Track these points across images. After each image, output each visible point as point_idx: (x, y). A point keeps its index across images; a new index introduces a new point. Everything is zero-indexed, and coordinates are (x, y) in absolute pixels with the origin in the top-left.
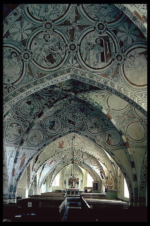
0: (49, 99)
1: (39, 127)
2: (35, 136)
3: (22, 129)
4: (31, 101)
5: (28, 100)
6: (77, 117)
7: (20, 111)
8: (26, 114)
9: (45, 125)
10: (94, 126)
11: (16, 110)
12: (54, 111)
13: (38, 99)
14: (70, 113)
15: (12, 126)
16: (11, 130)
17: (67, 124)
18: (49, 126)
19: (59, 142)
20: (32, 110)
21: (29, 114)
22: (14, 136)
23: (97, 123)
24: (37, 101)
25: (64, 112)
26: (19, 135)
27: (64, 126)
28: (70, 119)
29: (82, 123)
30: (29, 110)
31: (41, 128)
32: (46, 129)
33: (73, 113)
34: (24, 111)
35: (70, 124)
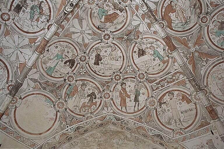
0: (137, 15)
1: (210, 62)
3: (184, 92)
4: (140, 48)
5: (135, 52)
7: (150, 74)
8: (160, 68)
11: (144, 78)
13: (138, 36)
15: (165, 102)
16: (168, 110)
20: (156, 54)
21: (162, 64)
22: (186, 114)
24: (142, 39)
26: (192, 106)
31: (216, 59)
34: (153, 69)
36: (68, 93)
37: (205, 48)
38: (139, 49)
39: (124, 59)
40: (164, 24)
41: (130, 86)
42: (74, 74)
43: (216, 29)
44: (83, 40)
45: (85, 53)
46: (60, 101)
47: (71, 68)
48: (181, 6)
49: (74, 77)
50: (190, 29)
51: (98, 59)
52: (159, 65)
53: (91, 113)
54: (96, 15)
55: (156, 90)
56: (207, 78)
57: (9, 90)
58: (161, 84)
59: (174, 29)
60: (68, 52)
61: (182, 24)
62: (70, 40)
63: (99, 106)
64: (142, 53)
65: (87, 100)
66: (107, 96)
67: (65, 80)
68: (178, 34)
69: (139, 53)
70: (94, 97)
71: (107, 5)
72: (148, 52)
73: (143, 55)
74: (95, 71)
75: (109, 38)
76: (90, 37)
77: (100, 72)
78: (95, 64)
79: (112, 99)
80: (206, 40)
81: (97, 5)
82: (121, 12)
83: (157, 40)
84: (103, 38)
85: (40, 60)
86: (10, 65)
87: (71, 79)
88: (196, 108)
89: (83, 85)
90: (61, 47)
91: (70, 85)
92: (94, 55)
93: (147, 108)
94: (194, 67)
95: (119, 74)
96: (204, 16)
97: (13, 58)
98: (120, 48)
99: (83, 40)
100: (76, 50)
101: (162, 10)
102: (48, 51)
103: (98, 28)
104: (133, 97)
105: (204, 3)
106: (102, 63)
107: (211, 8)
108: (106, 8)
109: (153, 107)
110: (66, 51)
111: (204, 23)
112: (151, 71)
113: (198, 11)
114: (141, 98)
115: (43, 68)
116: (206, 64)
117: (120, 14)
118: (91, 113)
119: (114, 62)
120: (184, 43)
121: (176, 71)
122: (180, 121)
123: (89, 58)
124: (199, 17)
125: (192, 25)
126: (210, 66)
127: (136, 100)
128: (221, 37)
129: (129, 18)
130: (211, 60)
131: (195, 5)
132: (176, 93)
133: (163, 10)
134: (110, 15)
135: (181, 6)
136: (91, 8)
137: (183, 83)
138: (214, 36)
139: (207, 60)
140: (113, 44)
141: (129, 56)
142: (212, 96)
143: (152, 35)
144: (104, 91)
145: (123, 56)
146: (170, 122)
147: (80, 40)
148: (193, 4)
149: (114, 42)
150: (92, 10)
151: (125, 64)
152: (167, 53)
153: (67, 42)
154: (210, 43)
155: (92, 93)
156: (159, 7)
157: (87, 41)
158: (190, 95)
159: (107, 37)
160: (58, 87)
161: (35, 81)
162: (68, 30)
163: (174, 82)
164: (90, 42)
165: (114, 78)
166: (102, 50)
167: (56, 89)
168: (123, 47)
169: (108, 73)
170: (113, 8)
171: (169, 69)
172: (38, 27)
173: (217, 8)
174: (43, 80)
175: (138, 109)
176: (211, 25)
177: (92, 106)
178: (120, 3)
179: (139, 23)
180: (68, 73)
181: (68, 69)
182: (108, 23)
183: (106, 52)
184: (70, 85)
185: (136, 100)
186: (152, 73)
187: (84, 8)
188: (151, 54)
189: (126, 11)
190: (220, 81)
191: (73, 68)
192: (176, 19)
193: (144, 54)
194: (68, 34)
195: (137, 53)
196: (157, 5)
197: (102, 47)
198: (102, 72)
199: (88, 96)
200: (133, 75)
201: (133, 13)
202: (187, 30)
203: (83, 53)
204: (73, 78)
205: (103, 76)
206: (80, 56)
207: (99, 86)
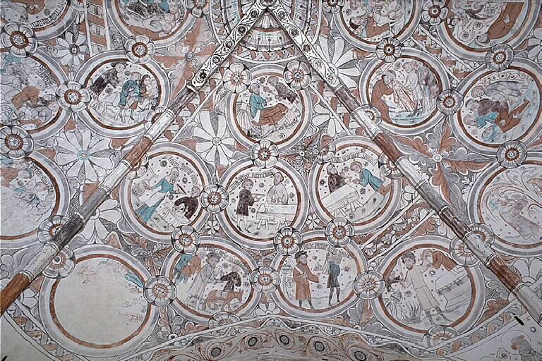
0: (321, 103)
1: (477, 177)
2: (519, 207)
3: (436, 246)
4: (333, 172)
7: (357, 225)
9: (479, 147)
11: (345, 235)
14: (450, 33)
15: (398, 278)
17: (510, 43)
18: (498, 129)
20: (366, 178)
21: (379, 197)
22: (448, 295)
24: (334, 152)
25: (444, 54)
26: (459, 272)
27: (518, 56)
30: (363, 191)
31: (486, 168)
32: (503, 145)
34: (364, 211)
35: (516, 27)
36: (179, 267)
37: (461, 152)
38: (331, 175)
39: (299, 200)
40: (375, 114)
41: (316, 258)
42: (194, 231)
43: (474, 115)
44: (217, 159)
45: (219, 186)
46: (160, 282)
47: (189, 217)
48: (403, 82)
49: (194, 238)
50: (425, 122)
51: (246, 202)
52: (375, 200)
53: (229, 314)
54: (244, 107)
55: (373, 256)
56: (479, 207)
57: (51, 234)
58: (383, 242)
59: (394, 122)
60: (185, 181)
61: (409, 113)
62: (192, 154)
63: (249, 300)
64: (336, 181)
65: (220, 286)
66: (264, 280)
67: (173, 241)
68: (404, 132)
69: (331, 182)
70: (236, 281)
71: (266, 89)
72: (349, 176)
73: (338, 185)
74: (240, 228)
75: (269, 156)
76: (230, 154)
77: (249, 232)
78: (239, 212)
79: (278, 287)
80: (460, 137)
81: (248, 86)
82: (292, 103)
83: (365, 147)
84: (256, 156)
85: (127, 182)
86: (65, 185)
87: (187, 241)
88: (470, 276)
89: (212, 255)
90: (172, 167)
91: (183, 252)
92: (237, 191)
93: (358, 295)
94: (447, 188)
95: (290, 233)
96: (447, 95)
97: (73, 173)
98: (291, 178)
99: (217, 159)
100: (202, 179)
101: (367, 91)
102: (146, 166)
103: (248, 136)
104: (324, 279)
105: (443, 73)
106: (253, 211)
107: (456, 80)
108: (264, 95)
109: (372, 292)
110: (181, 178)
111: (449, 107)
112: (359, 216)
113: (435, 88)
114: (344, 279)
115: (130, 202)
116: (471, 181)
117: (290, 107)
118: (229, 314)
119: (279, 208)
120: (417, 148)
121: (411, 205)
122: (440, 311)
123: (227, 199)
124: (439, 99)
125: (426, 115)
126: (478, 185)
127: (332, 283)
128: (487, 126)
129: (307, 112)
130: (479, 173)
131: (427, 79)
132: (418, 253)
133: (370, 91)
134: (272, 109)
135: (403, 82)
136: (235, 92)
137: (430, 228)
138: (475, 128)
139: (471, 174)
140: (278, 168)
141: (311, 193)
142: (496, 241)
143: (353, 139)
144: (257, 270)
145: (299, 194)
146: (417, 316)
147: (210, 158)
148: (424, 77)
149: (279, 164)
150: (237, 97)
151: (302, 211)
152: (387, 169)
153: (185, 158)
154: (470, 141)
155: (233, 273)
156: (362, 86)
157: (224, 162)
158: (450, 250)
159: (264, 155)
160: (158, 252)
161: (110, 227)
162: (189, 131)
163: (411, 232)
164: (230, 164)
165: (279, 242)
166: (254, 182)
167: (151, 254)
168: (296, 175)
169: (266, 233)
170: (277, 94)
171: (396, 204)
172: (132, 119)
173: (469, 78)
174: (128, 229)
175: (338, 301)
176: (464, 108)
177: (230, 300)
178: (289, 84)
179: (327, 118)
180: (180, 227)
181: (178, 219)
182: (267, 125)
183: (262, 186)
184: (183, 252)
185: (332, 283)
186: (361, 221)
187: (223, 91)
188: (355, 182)
189: (302, 99)
190: (506, 209)
191: (193, 218)
192: (396, 105)
193: (341, 184)
194: (190, 141)
195: (327, 184)
196: (357, 82)
197: (256, 176)
198: (253, 230)
199: (223, 278)
200: (321, 233)
201: (314, 99)
202: (420, 124)
203: (215, 187)
204: (192, 240)
205: (257, 240)
206: (209, 192)
207: (248, 260)
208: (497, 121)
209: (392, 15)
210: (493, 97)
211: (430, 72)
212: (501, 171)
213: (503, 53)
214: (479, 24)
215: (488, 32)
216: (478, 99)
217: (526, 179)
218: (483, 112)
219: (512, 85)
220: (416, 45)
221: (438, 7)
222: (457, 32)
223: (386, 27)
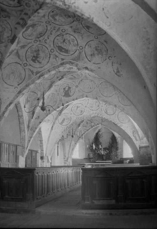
0: (21, 14)
2: (12, 73)
6: (69, 41)
10: (96, 52)
12: (35, 34)
14: (58, 36)
18: (31, 58)
19: (64, 89)
23: (99, 47)
24: (5, 20)
25: (51, 35)
28: (60, 45)
29: (78, 50)
32: (27, 61)
33: (63, 35)
35: (61, 53)
124: (36, 38)
201: (22, 11)
208: (34, 57)
209: (60, 20)
210: (40, 52)
211: (43, 34)
212: (20, 64)
213: (54, 52)
214: (61, 43)
215: (59, 46)
216: (39, 48)
217: (20, 71)
218: (35, 51)
219: (45, 57)
220: (51, 28)
221: (65, 31)
222: (58, 37)
223: (55, 20)
